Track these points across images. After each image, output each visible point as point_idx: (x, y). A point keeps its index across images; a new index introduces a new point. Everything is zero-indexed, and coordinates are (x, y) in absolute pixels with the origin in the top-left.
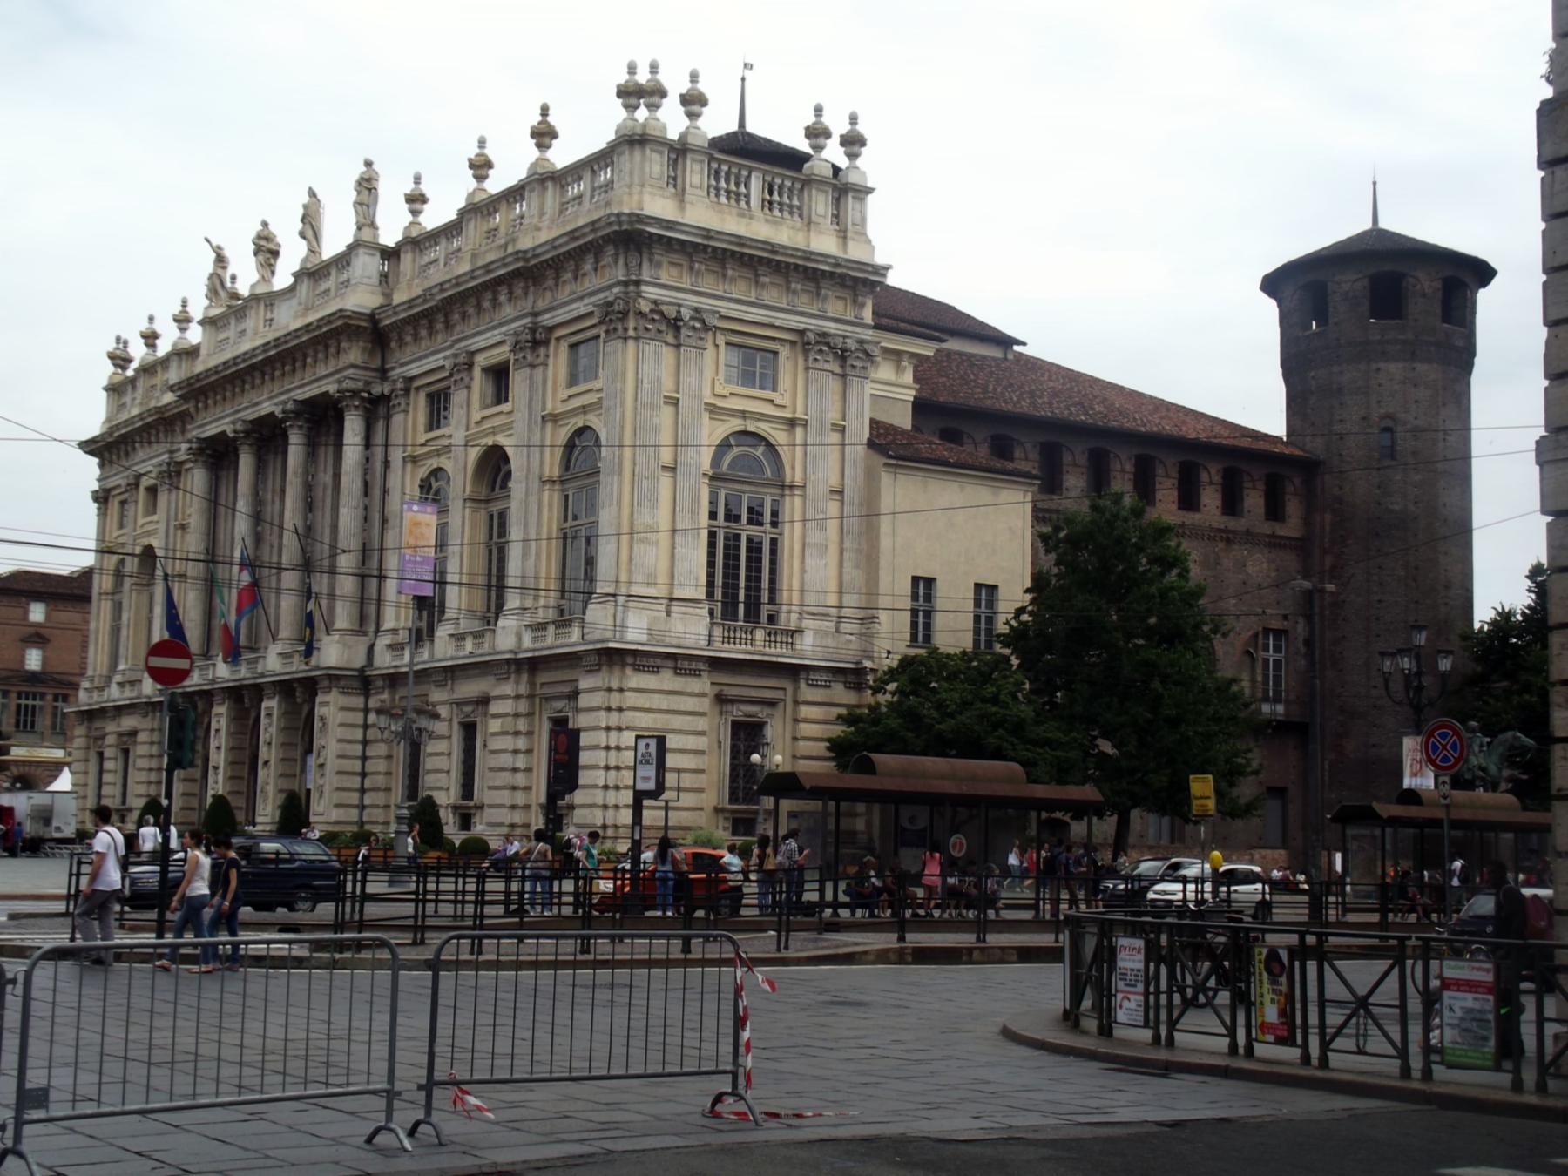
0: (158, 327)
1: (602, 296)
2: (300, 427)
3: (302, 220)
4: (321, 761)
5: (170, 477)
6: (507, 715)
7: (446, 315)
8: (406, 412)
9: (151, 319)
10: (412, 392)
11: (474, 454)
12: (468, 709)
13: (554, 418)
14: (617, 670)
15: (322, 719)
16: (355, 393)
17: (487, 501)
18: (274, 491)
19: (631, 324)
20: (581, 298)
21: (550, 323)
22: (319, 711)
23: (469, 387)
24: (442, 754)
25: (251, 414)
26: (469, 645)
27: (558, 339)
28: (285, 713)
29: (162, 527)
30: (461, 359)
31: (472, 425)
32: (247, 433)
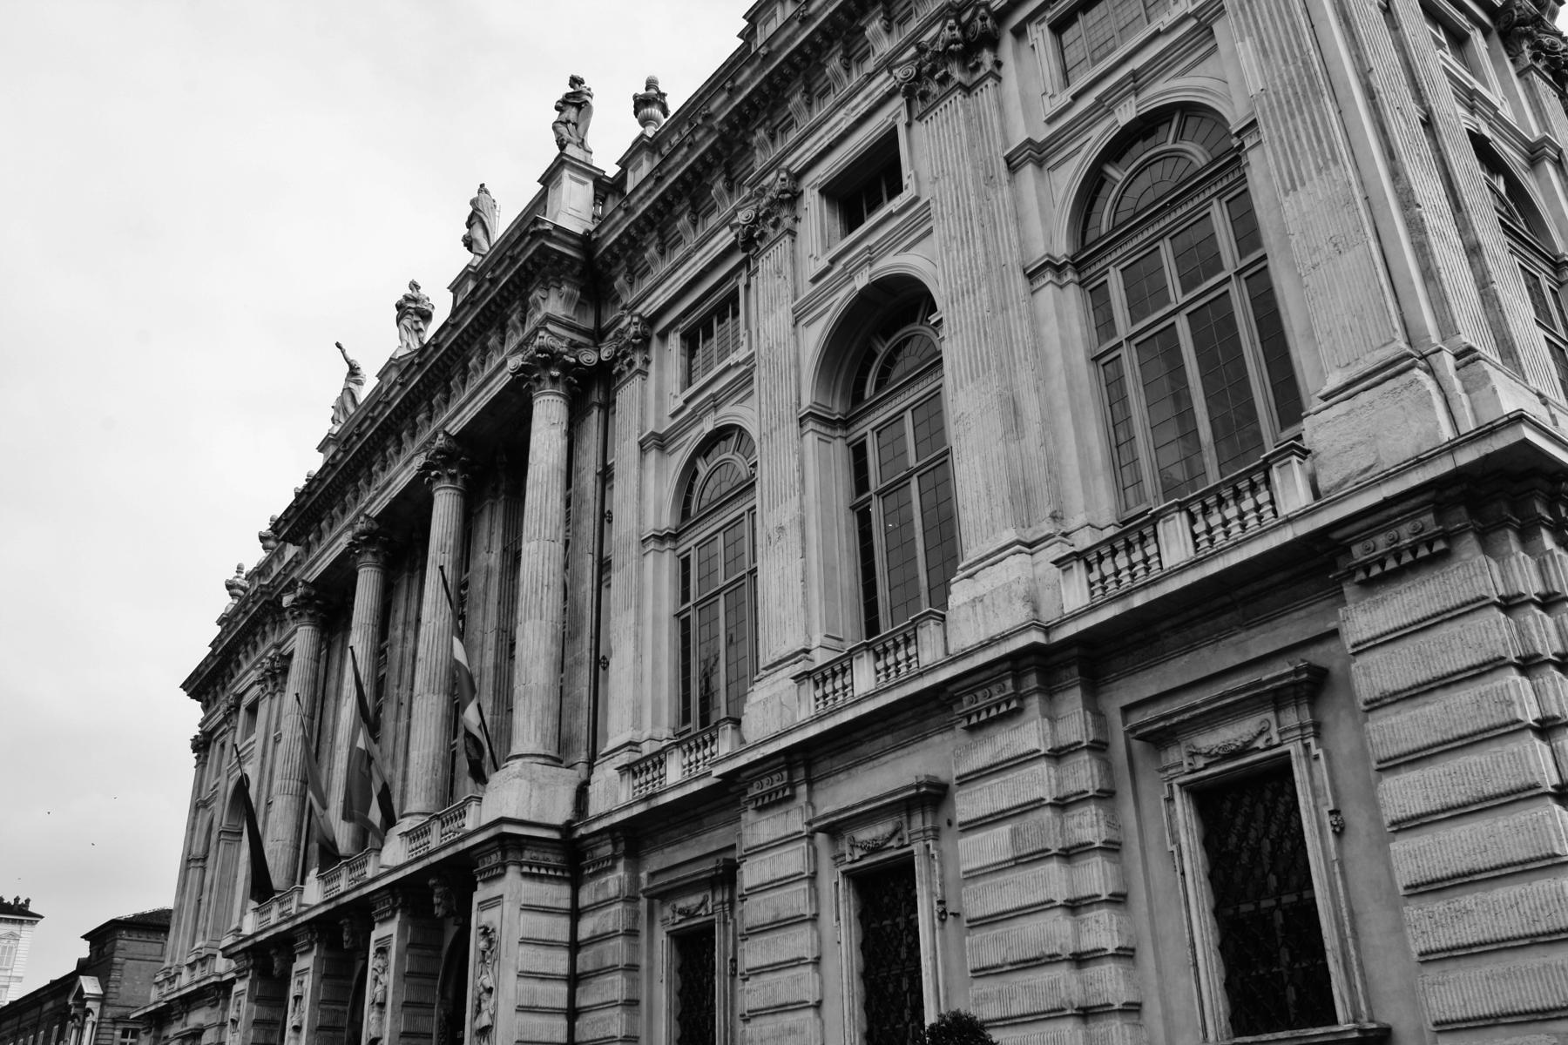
2: (453, 477)
3: (469, 225)
4: (484, 1020)
6: (1037, 804)
7: (729, 171)
8: (644, 373)
10: (655, 341)
11: (814, 336)
12: (865, 835)
13: (1037, 154)
17: (846, 423)
18: (406, 623)
22: (478, 919)
23: (792, 233)
24: (798, 962)
26: (864, 676)
28: (411, 945)
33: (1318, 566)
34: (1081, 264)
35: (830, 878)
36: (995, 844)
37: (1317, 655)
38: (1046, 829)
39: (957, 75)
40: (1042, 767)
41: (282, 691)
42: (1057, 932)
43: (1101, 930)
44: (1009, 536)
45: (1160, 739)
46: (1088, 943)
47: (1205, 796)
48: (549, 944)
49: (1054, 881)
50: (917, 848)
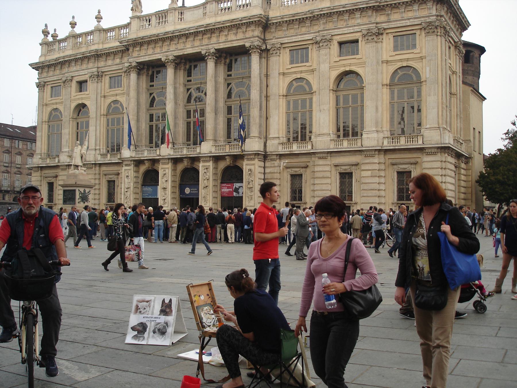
0: (75, 20)
1: (423, 19)
5: (97, 77)
9: (73, 17)
11: (335, 74)
13: (387, 62)
14: (443, 154)
15: (250, 170)
16: (259, 47)
19: (439, 31)
20: (409, 19)
21: (385, 27)
25: (177, 53)
27: (387, 33)
29: (93, 97)
30: (329, 37)
31: (332, 62)
32: (174, 60)
33: (421, 150)
34: (391, 85)
35: (334, 172)
36: (369, 173)
37: (418, 160)
38: (377, 173)
39: (375, 39)
40: (377, 165)
41: (101, 82)
42: (377, 186)
43: (382, 187)
44: (374, 129)
45: (393, 164)
46: (381, 188)
47: (398, 173)
48: (261, 173)
49: (377, 180)
50: (353, 171)
